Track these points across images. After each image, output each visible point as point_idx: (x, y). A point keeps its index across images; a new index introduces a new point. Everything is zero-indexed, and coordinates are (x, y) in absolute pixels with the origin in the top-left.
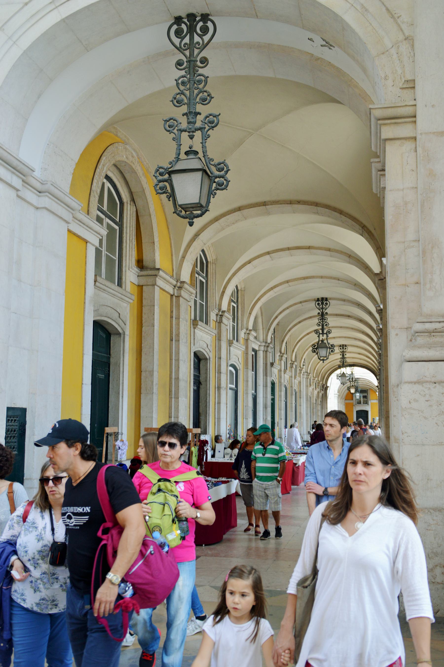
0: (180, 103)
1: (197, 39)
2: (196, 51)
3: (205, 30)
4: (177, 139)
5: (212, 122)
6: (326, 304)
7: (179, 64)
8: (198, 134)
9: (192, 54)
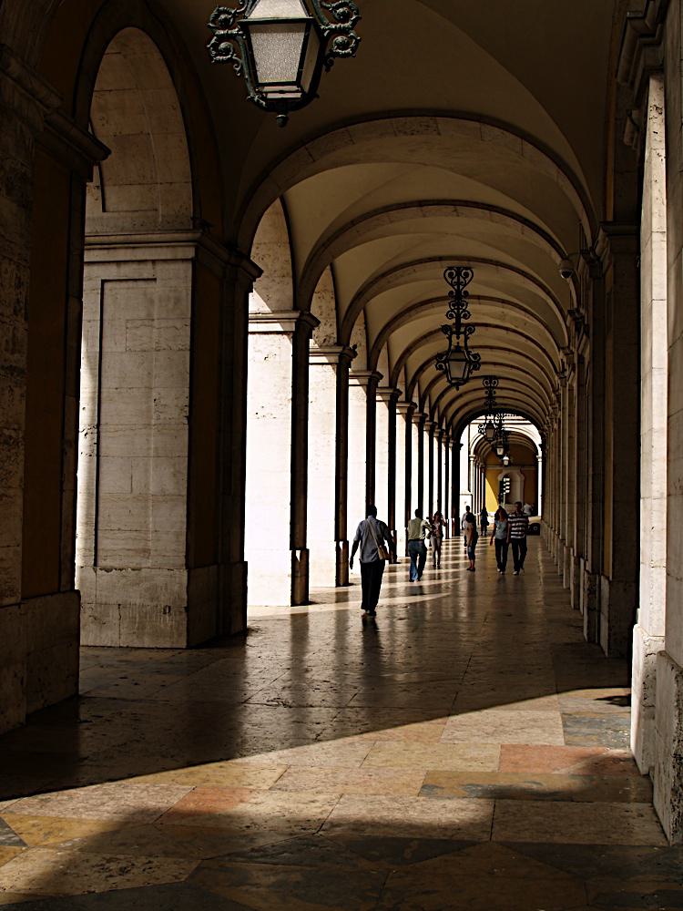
0: (452, 317)
1: (462, 280)
2: (461, 287)
3: (467, 275)
4: (450, 338)
5: (471, 328)
6: (495, 383)
7: (451, 293)
8: (462, 336)
9: (459, 287)
